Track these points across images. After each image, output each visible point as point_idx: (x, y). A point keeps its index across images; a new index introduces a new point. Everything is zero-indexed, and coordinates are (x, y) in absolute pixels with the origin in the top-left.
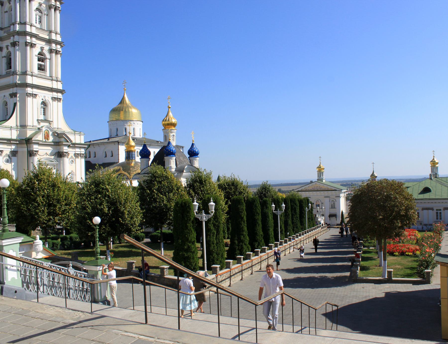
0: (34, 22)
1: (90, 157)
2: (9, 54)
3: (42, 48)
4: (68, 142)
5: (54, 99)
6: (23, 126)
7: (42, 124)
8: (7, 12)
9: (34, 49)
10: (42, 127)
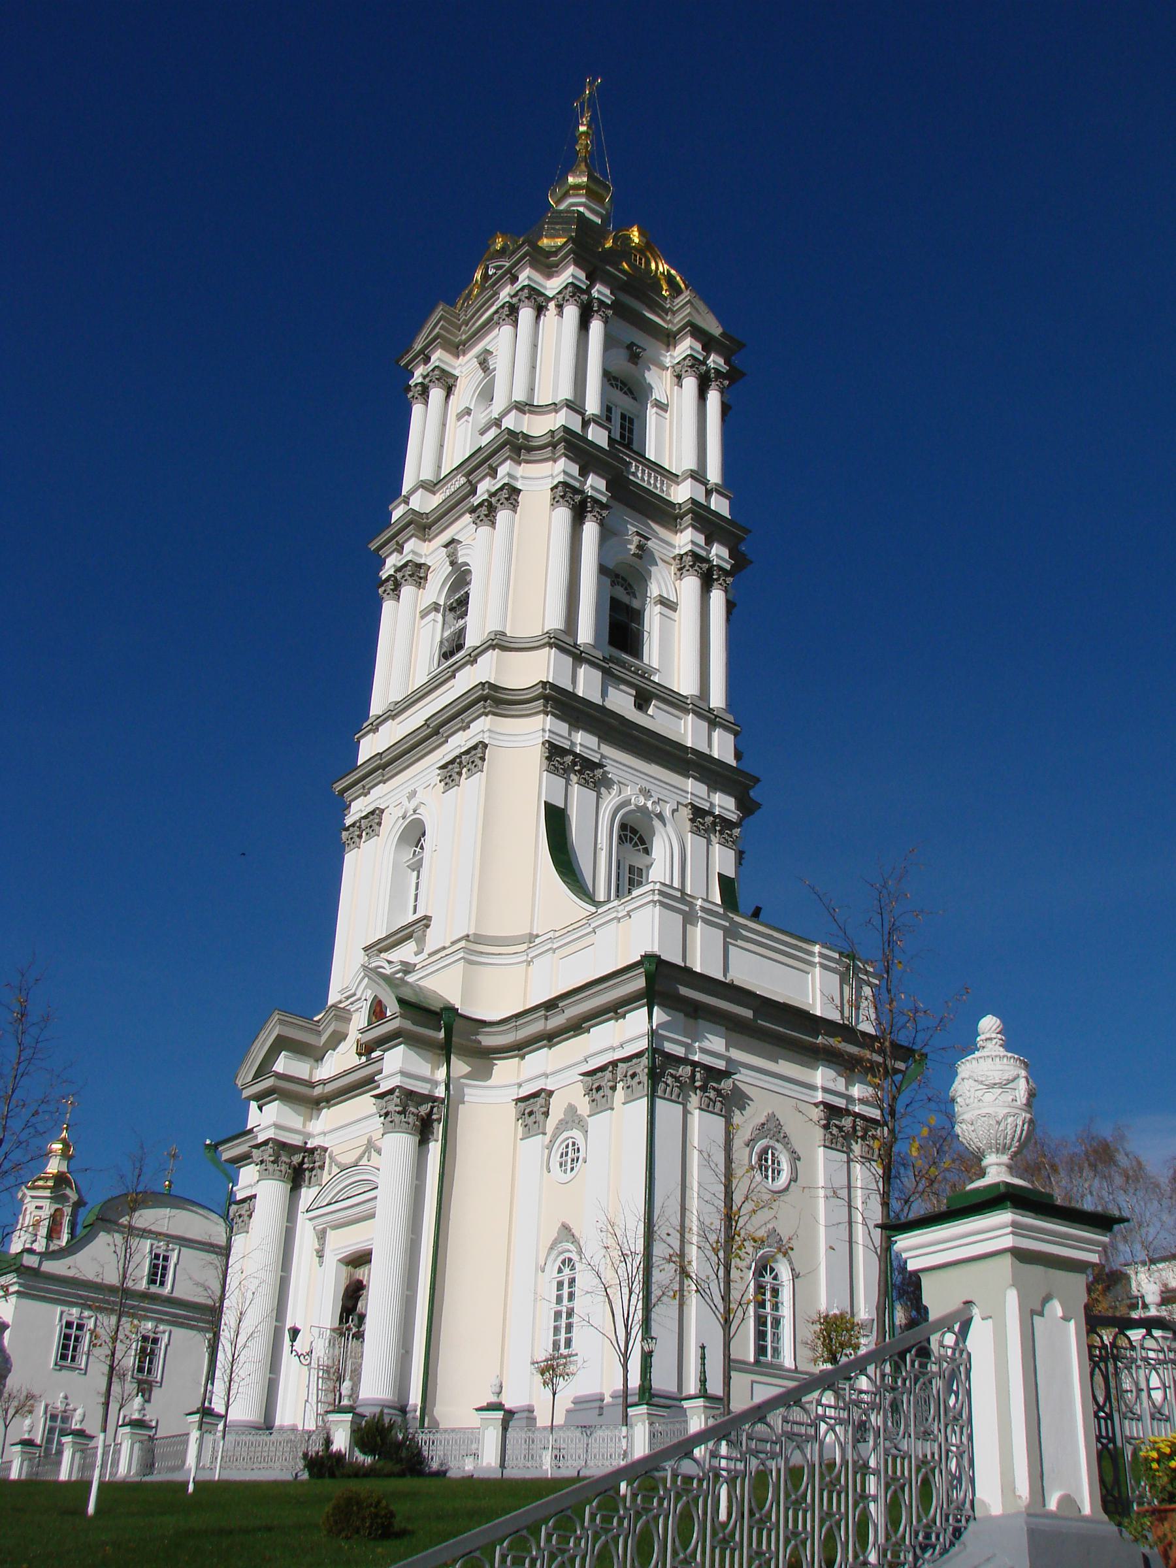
2: (461, 578)
8: (468, 411)
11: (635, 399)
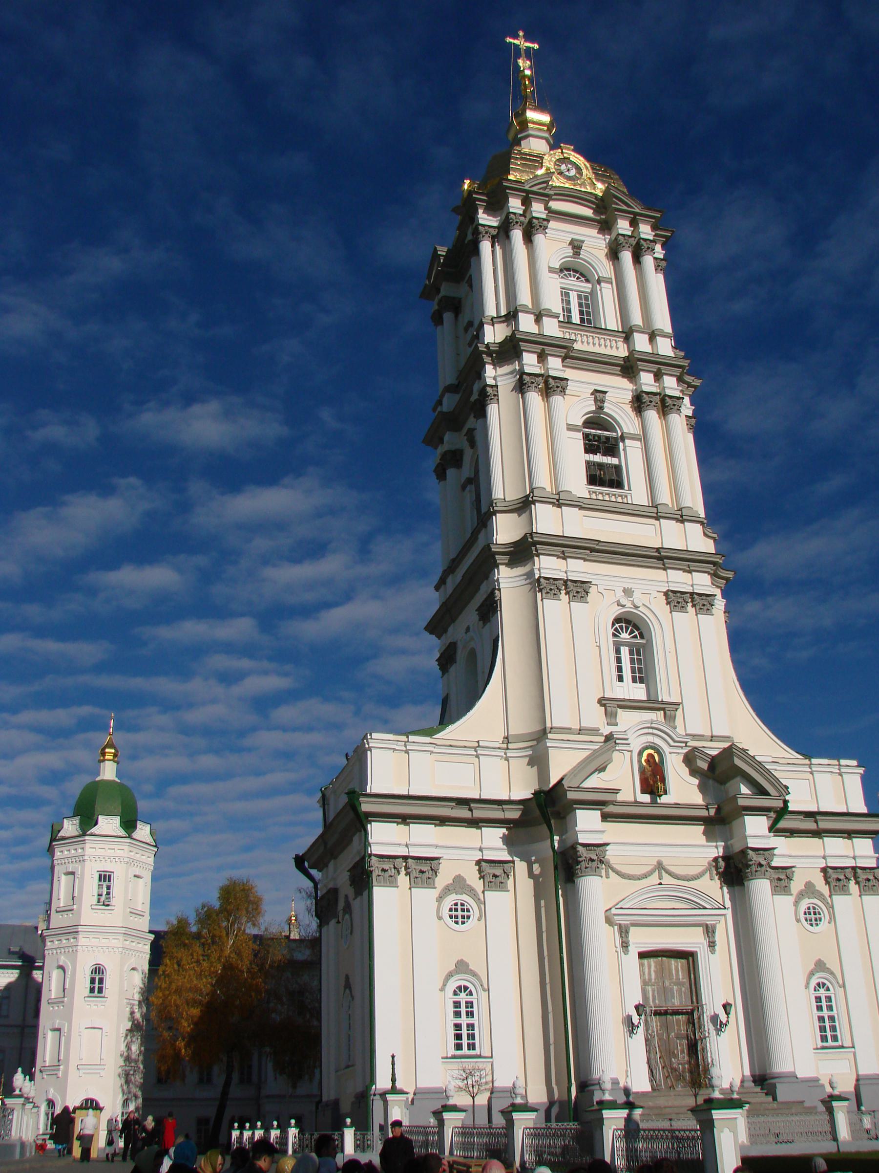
0: (552, 301)
3: (599, 396)
4: (763, 792)
5: (676, 600)
6: (537, 745)
7: (627, 720)
9: (556, 399)
11: (587, 281)
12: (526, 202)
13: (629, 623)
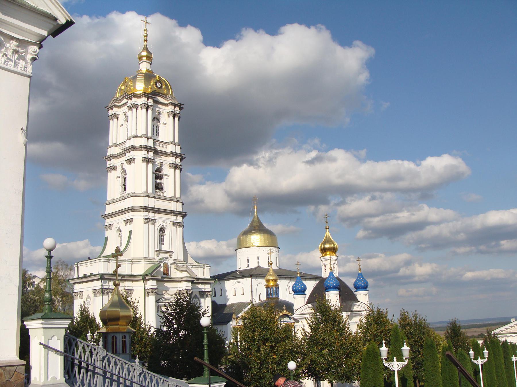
1: (215, 296)
5: (175, 224)
8: (122, 125)
9: (150, 166)
10: (160, 259)
12: (148, 99)
13: (162, 230)
